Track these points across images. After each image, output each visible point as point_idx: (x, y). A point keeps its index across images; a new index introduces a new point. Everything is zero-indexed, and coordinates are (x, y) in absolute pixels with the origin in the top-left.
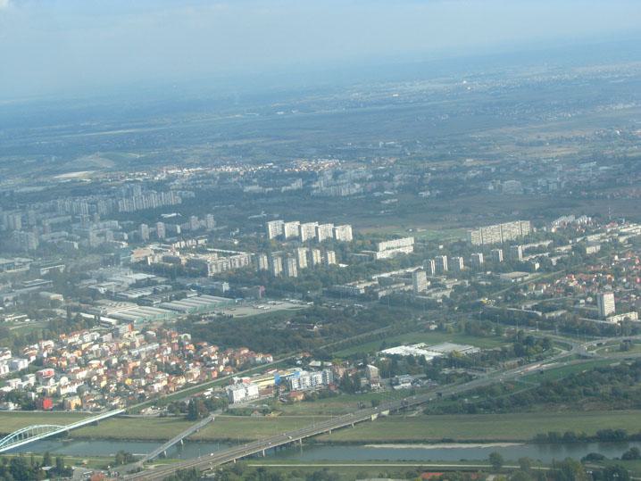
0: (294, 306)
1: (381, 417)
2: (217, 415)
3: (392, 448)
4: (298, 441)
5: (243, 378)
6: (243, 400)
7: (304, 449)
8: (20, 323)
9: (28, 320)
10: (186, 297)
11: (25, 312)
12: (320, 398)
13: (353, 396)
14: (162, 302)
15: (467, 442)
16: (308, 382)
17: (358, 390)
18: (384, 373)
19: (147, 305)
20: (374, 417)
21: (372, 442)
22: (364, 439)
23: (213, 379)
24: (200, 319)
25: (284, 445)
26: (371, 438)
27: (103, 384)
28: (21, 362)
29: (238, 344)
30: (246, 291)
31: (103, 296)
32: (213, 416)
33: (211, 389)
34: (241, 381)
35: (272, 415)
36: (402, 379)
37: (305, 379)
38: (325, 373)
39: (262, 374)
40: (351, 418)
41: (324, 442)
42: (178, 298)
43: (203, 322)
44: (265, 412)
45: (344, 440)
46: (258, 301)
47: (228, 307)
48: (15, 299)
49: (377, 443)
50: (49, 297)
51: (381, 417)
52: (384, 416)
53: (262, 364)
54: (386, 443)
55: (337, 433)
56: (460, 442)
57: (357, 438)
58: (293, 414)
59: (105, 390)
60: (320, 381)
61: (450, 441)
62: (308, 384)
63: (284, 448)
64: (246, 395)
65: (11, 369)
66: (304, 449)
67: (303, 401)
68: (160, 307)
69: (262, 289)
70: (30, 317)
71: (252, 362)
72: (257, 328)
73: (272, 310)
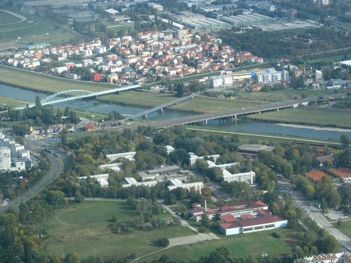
0: (312, 25)
1: (300, 106)
2: (196, 95)
3: (293, 127)
4: (234, 117)
5: (227, 72)
6: (220, 87)
7: (239, 122)
8: (124, 23)
9: (129, 21)
10: (242, 14)
11: (130, 16)
12: (272, 90)
13: (296, 91)
14: (224, 16)
15: (345, 128)
16: (270, 78)
17: (302, 86)
18: (326, 77)
19: (212, 18)
20: (295, 106)
21: (282, 122)
22: (278, 119)
23: (216, 71)
24: (238, 30)
25: (225, 118)
26: (283, 119)
27: (141, 68)
28: (102, 49)
29: (244, 48)
30: (284, 13)
31: (188, 9)
32: (193, 95)
33: (207, 78)
34: (225, 74)
35: (232, 98)
36: (335, 82)
37: (271, 76)
38: (283, 73)
39: (248, 70)
40: (278, 105)
41: (252, 119)
42: (235, 14)
43: (241, 32)
44: (230, 95)
45: (265, 119)
46: (289, 20)
47: (264, 23)
48: (131, 6)
49: (286, 123)
50: (152, 6)
51: (300, 106)
52: (303, 106)
53: (254, 64)
54: (291, 123)
55: (264, 114)
56: (341, 127)
57: (274, 119)
58: (247, 99)
59: (140, 72)
60: (279, 78)
61: (334, 126)
62: (270, 80)
63: (225, 121)
64: (223, 83)
65: (93, 52)
66: (239, 122)
67: (260, 91)
68: (221, 20)
69: (295, 11)
70: (131, 20)
71: (249, 62)
72: (271, 39)
73: (294, 27)
